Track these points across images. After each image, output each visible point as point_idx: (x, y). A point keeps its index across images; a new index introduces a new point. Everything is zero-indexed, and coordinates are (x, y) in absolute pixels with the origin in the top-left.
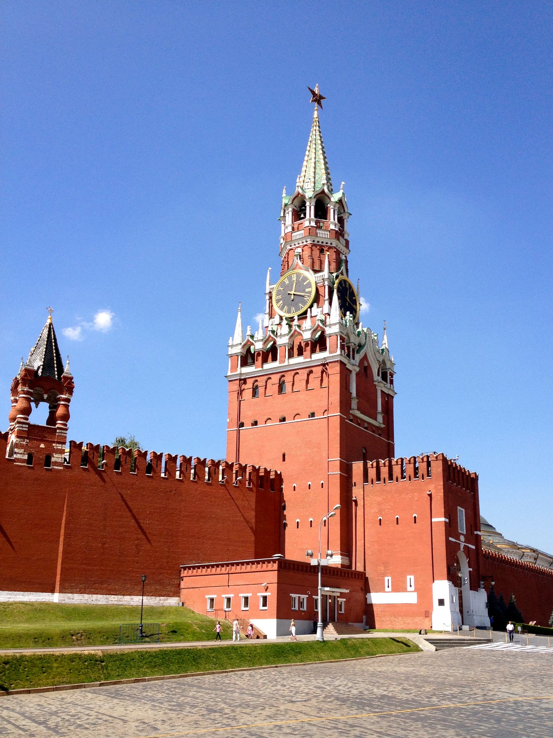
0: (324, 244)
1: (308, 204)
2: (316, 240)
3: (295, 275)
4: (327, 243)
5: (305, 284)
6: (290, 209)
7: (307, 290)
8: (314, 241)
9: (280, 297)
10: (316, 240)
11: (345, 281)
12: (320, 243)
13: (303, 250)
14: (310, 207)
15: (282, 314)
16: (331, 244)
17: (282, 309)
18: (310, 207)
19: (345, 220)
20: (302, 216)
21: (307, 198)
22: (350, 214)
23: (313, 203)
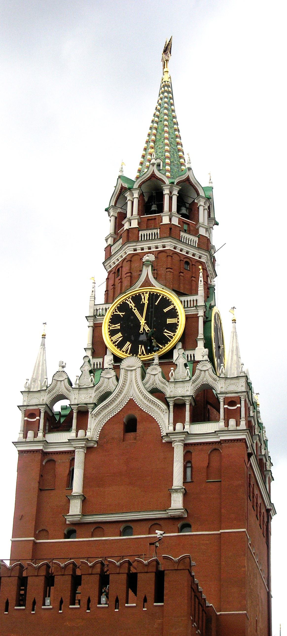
0: (190, 255)
1: (166, 192)
3: (147, 296)
4: (194, 255)
5: (165, 310)
6: (136, 195)
7: (169, 321)
8: (175, 248)
9: (118, 326)
13: (156, 257)
14: (171, 198)
15: (119, 353)
17: (120, 346)
18: (171, 198)
20: (154, 208)
21: (167, 181)
22: (217, 224)
23: (175, 192)
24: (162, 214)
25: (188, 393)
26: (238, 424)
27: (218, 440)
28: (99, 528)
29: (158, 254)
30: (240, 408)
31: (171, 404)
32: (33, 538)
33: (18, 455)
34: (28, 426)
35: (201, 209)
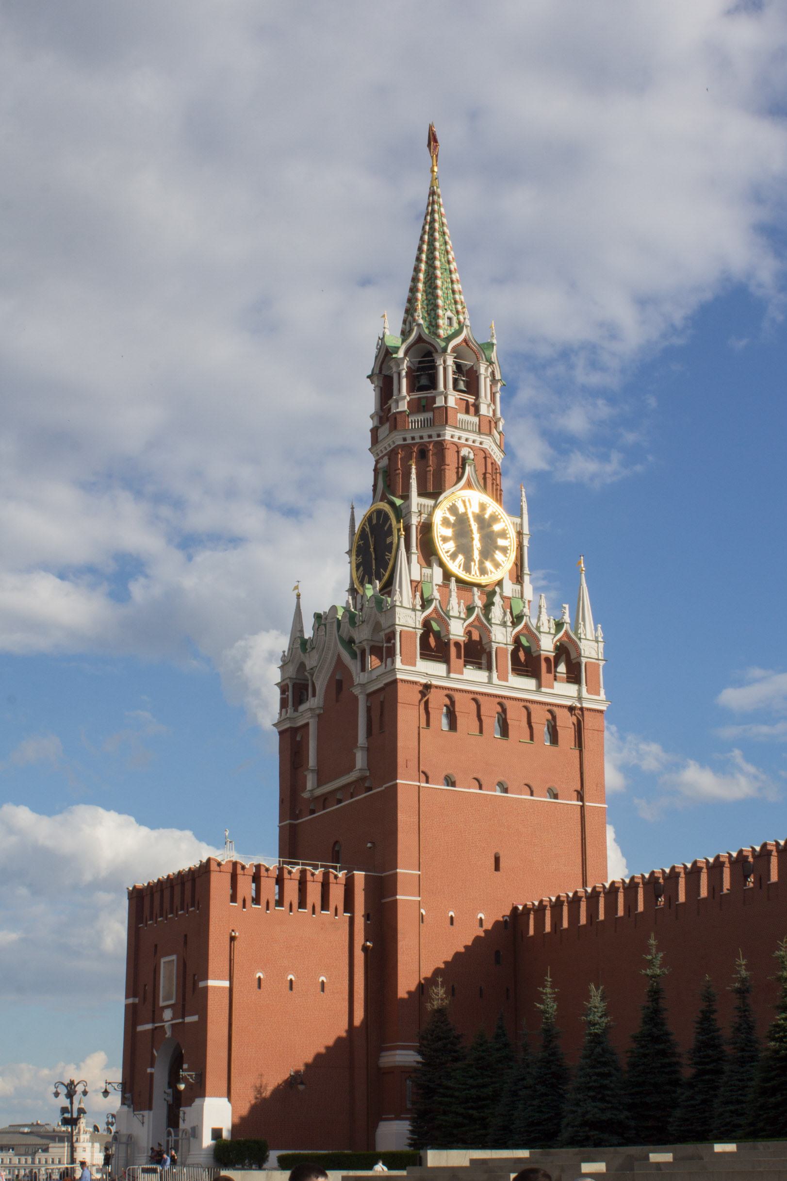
0: (426, 439)
1: (394, 370)
2: (408, 436)
8: (405, 439)
10: (408, 436)
12: (417, 440)
13: (389, 459)
18: (399, 374)
19: (482, 378)
24: (390, 402)
25: (365, 637)
26: (393, 662)
27: (381, 685)
28: (324, 800)
29: (392, 454)
30: (394, 644)
31: (358, 652)
32: (288, 822)
33: (278, 737)
34: (284, 704)
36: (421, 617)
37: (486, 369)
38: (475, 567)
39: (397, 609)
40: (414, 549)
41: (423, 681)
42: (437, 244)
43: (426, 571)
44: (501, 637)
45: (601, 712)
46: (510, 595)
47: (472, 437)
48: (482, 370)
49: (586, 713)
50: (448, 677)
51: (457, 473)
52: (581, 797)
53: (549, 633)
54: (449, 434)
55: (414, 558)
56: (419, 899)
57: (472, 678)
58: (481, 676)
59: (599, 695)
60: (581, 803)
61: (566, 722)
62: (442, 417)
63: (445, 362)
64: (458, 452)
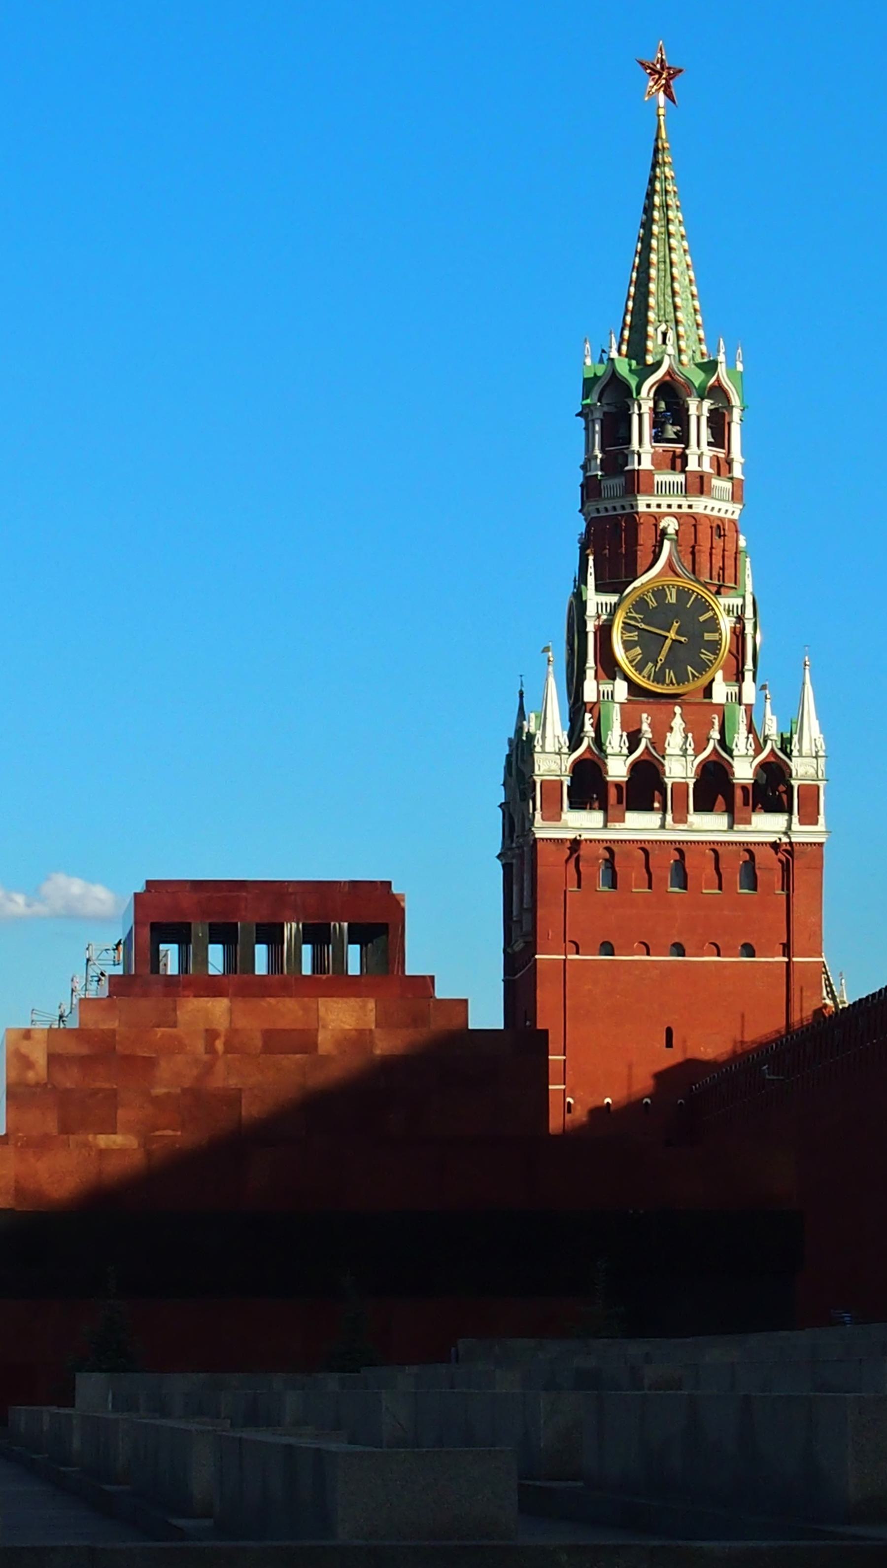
8: (598, 511)
11: (659, 594)
16: (632, 507)
35: (635, 419)
36: (568, 761)
37: (699, 408)
38: (670, 675)
39: (536, 756)
40: (591, 662)
41: (571, 836)
42: (655, 229)
43: (606, 687)
44: (680, 769)
45: (821, 845)
46: (723, 701)
47: (675, 501)
48: (693, 411)
49: (796, 848)
50: (605, 826)
51: (654, 552)
52: (787, 950)
53: (746, 755)
54: (642, 503)
55: (590, 674)
56: (563, 1087)
57: (640, 825)
58: (651, 820)
59: (816, 823)
60: (786, 959)
61: (768, 861)
62: (634, 483)
63: (640, 408)
64: (656, 526)
